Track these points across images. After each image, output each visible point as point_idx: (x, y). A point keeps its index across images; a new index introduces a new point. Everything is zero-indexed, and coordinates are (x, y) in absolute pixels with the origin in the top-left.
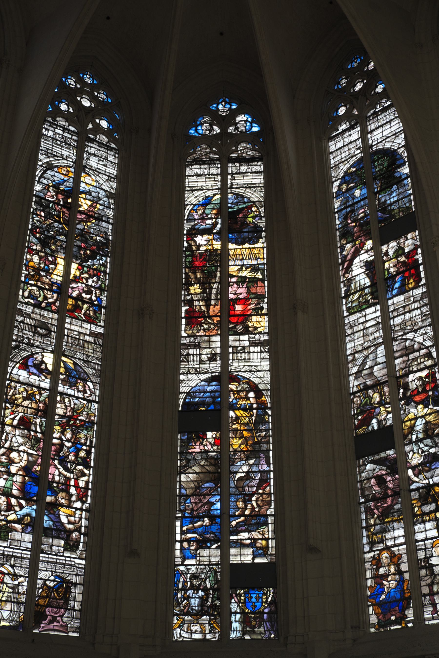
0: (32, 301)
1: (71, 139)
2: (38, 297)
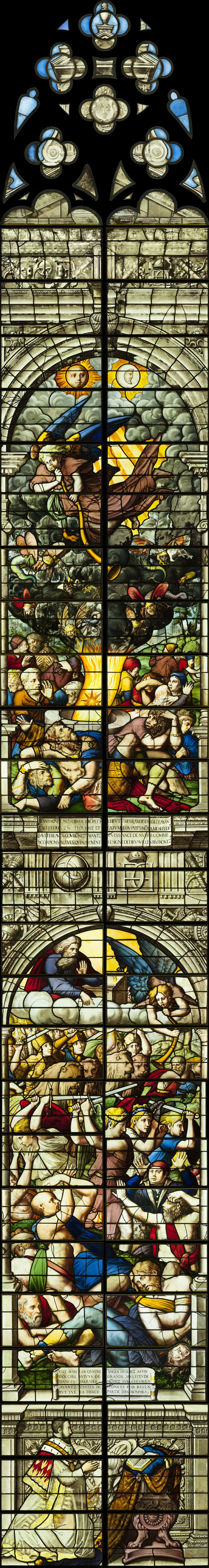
0: (34, 802)
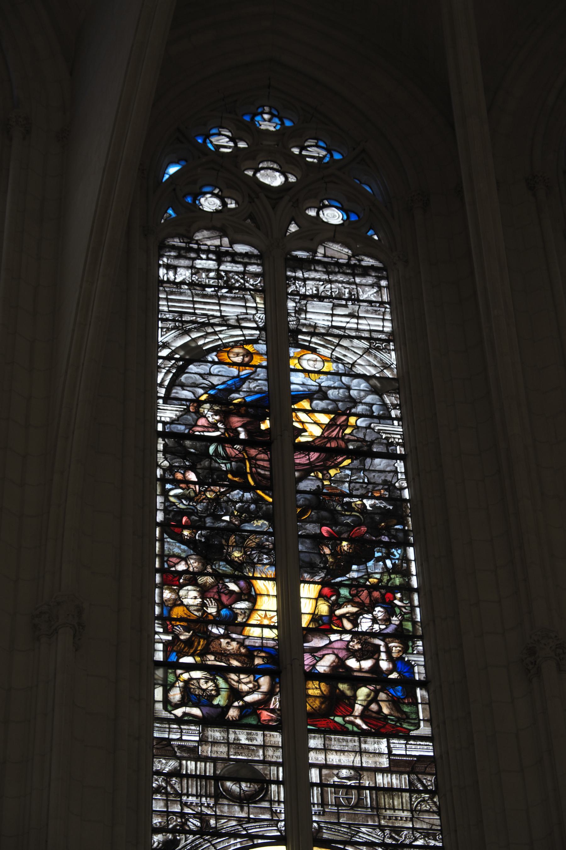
0: (196, 711)
1: (244, 273)
2: (213, 697)
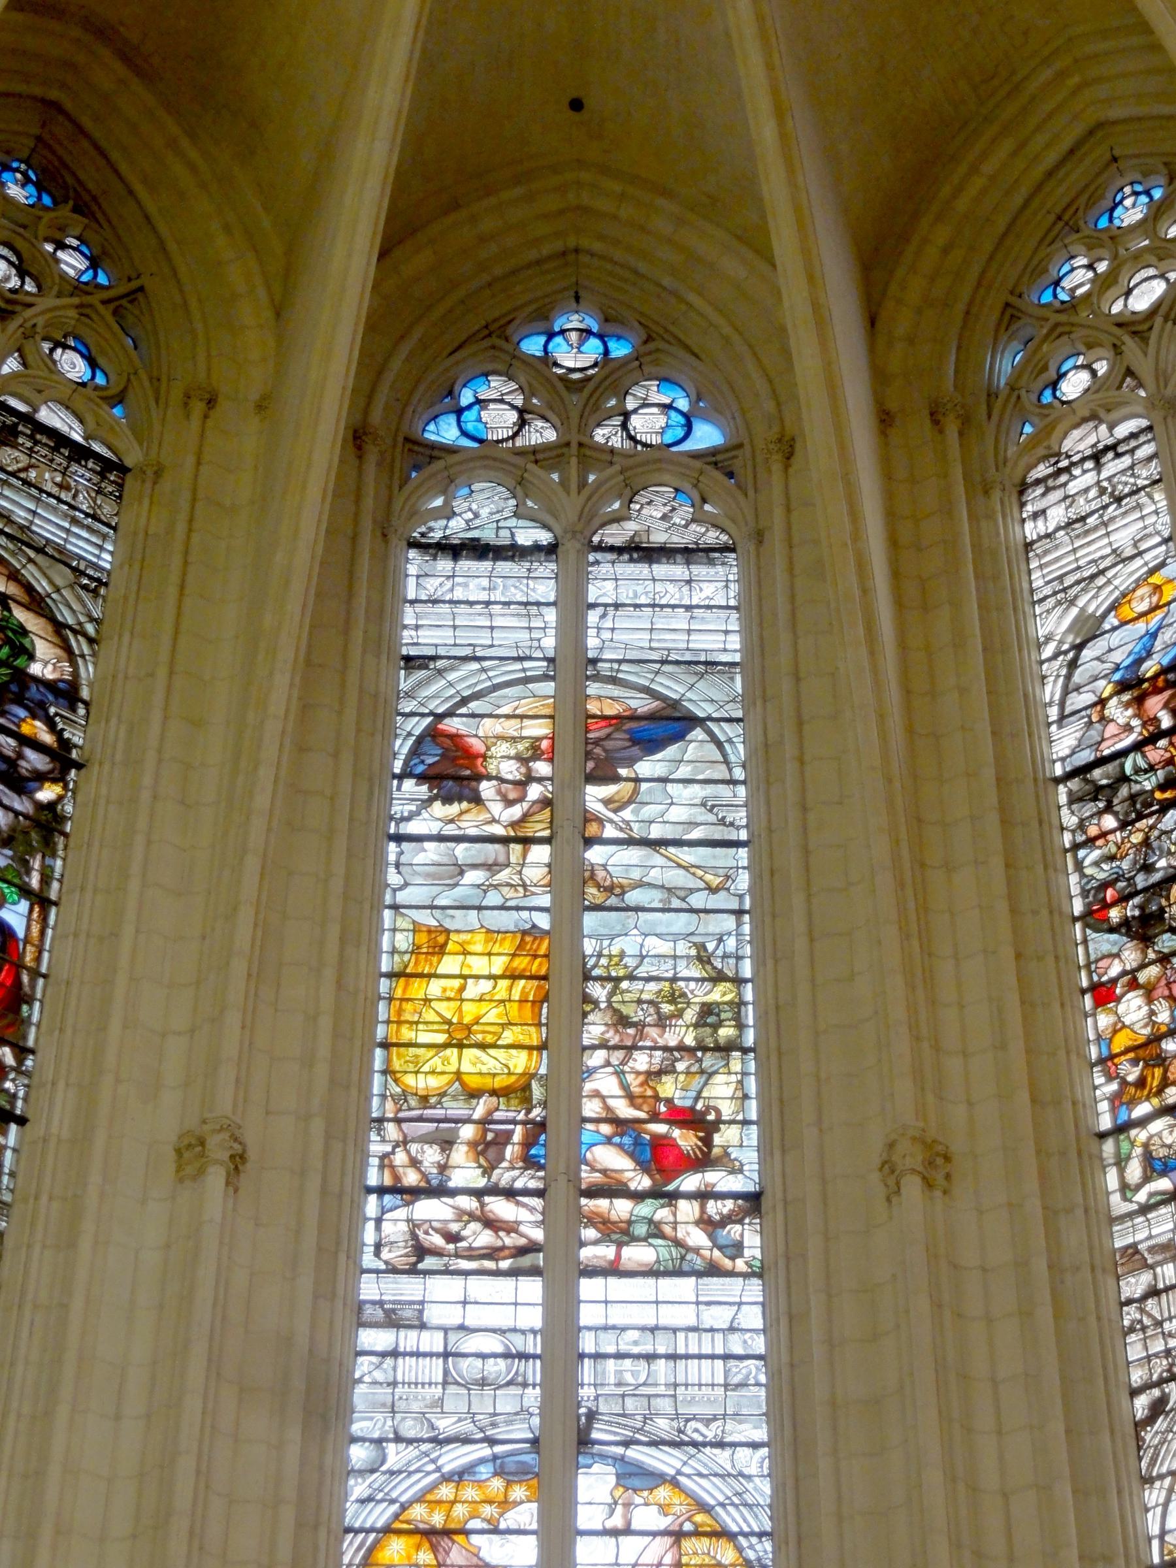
1: (1132, 467)
